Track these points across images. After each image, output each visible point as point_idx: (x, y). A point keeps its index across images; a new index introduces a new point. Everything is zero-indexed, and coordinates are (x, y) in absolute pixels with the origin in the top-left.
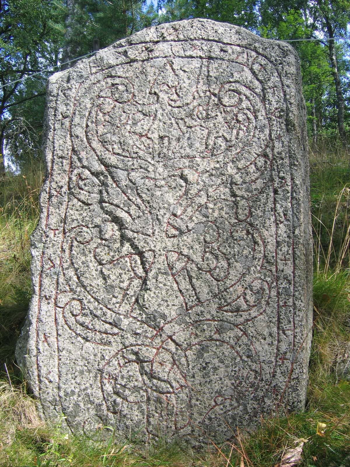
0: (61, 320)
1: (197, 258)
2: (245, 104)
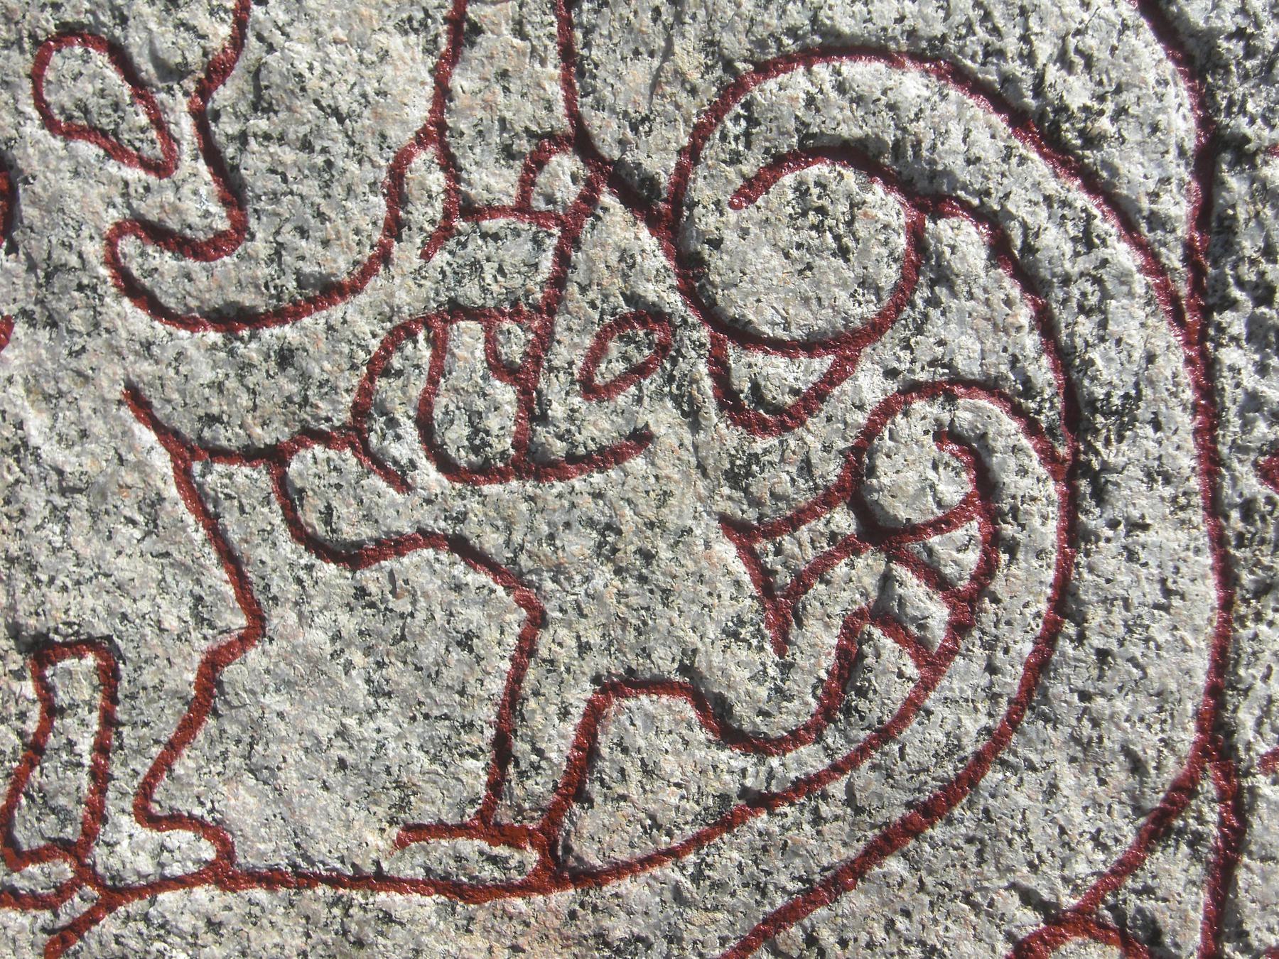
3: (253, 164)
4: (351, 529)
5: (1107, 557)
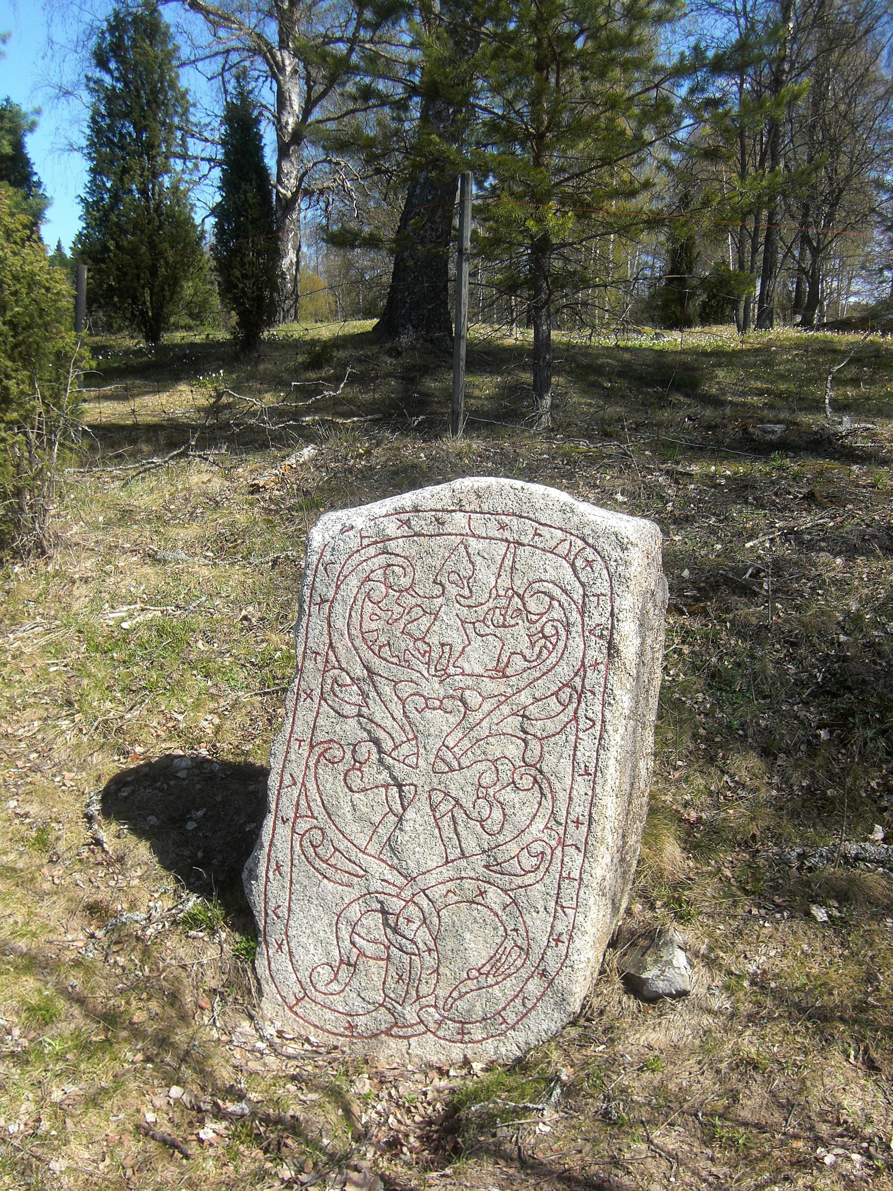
0: (297, 848)
1: (467, 802)
2: (557, 614)
3: (474, 589)
4: (482, 633)
5: (571, 641)
